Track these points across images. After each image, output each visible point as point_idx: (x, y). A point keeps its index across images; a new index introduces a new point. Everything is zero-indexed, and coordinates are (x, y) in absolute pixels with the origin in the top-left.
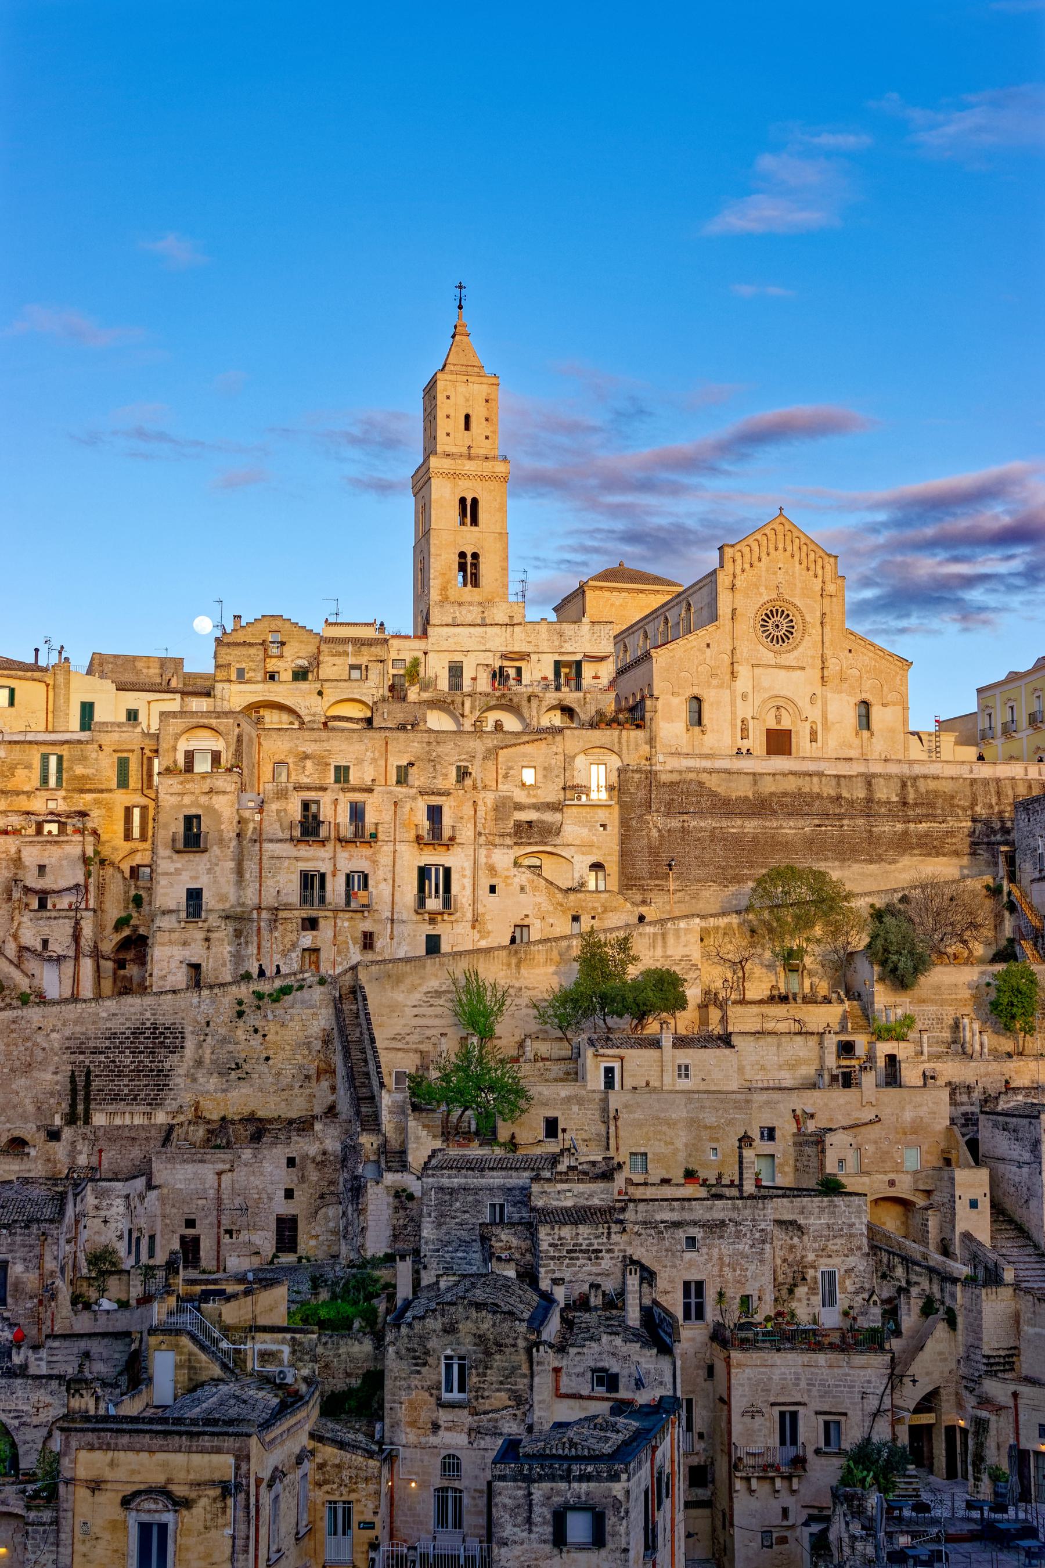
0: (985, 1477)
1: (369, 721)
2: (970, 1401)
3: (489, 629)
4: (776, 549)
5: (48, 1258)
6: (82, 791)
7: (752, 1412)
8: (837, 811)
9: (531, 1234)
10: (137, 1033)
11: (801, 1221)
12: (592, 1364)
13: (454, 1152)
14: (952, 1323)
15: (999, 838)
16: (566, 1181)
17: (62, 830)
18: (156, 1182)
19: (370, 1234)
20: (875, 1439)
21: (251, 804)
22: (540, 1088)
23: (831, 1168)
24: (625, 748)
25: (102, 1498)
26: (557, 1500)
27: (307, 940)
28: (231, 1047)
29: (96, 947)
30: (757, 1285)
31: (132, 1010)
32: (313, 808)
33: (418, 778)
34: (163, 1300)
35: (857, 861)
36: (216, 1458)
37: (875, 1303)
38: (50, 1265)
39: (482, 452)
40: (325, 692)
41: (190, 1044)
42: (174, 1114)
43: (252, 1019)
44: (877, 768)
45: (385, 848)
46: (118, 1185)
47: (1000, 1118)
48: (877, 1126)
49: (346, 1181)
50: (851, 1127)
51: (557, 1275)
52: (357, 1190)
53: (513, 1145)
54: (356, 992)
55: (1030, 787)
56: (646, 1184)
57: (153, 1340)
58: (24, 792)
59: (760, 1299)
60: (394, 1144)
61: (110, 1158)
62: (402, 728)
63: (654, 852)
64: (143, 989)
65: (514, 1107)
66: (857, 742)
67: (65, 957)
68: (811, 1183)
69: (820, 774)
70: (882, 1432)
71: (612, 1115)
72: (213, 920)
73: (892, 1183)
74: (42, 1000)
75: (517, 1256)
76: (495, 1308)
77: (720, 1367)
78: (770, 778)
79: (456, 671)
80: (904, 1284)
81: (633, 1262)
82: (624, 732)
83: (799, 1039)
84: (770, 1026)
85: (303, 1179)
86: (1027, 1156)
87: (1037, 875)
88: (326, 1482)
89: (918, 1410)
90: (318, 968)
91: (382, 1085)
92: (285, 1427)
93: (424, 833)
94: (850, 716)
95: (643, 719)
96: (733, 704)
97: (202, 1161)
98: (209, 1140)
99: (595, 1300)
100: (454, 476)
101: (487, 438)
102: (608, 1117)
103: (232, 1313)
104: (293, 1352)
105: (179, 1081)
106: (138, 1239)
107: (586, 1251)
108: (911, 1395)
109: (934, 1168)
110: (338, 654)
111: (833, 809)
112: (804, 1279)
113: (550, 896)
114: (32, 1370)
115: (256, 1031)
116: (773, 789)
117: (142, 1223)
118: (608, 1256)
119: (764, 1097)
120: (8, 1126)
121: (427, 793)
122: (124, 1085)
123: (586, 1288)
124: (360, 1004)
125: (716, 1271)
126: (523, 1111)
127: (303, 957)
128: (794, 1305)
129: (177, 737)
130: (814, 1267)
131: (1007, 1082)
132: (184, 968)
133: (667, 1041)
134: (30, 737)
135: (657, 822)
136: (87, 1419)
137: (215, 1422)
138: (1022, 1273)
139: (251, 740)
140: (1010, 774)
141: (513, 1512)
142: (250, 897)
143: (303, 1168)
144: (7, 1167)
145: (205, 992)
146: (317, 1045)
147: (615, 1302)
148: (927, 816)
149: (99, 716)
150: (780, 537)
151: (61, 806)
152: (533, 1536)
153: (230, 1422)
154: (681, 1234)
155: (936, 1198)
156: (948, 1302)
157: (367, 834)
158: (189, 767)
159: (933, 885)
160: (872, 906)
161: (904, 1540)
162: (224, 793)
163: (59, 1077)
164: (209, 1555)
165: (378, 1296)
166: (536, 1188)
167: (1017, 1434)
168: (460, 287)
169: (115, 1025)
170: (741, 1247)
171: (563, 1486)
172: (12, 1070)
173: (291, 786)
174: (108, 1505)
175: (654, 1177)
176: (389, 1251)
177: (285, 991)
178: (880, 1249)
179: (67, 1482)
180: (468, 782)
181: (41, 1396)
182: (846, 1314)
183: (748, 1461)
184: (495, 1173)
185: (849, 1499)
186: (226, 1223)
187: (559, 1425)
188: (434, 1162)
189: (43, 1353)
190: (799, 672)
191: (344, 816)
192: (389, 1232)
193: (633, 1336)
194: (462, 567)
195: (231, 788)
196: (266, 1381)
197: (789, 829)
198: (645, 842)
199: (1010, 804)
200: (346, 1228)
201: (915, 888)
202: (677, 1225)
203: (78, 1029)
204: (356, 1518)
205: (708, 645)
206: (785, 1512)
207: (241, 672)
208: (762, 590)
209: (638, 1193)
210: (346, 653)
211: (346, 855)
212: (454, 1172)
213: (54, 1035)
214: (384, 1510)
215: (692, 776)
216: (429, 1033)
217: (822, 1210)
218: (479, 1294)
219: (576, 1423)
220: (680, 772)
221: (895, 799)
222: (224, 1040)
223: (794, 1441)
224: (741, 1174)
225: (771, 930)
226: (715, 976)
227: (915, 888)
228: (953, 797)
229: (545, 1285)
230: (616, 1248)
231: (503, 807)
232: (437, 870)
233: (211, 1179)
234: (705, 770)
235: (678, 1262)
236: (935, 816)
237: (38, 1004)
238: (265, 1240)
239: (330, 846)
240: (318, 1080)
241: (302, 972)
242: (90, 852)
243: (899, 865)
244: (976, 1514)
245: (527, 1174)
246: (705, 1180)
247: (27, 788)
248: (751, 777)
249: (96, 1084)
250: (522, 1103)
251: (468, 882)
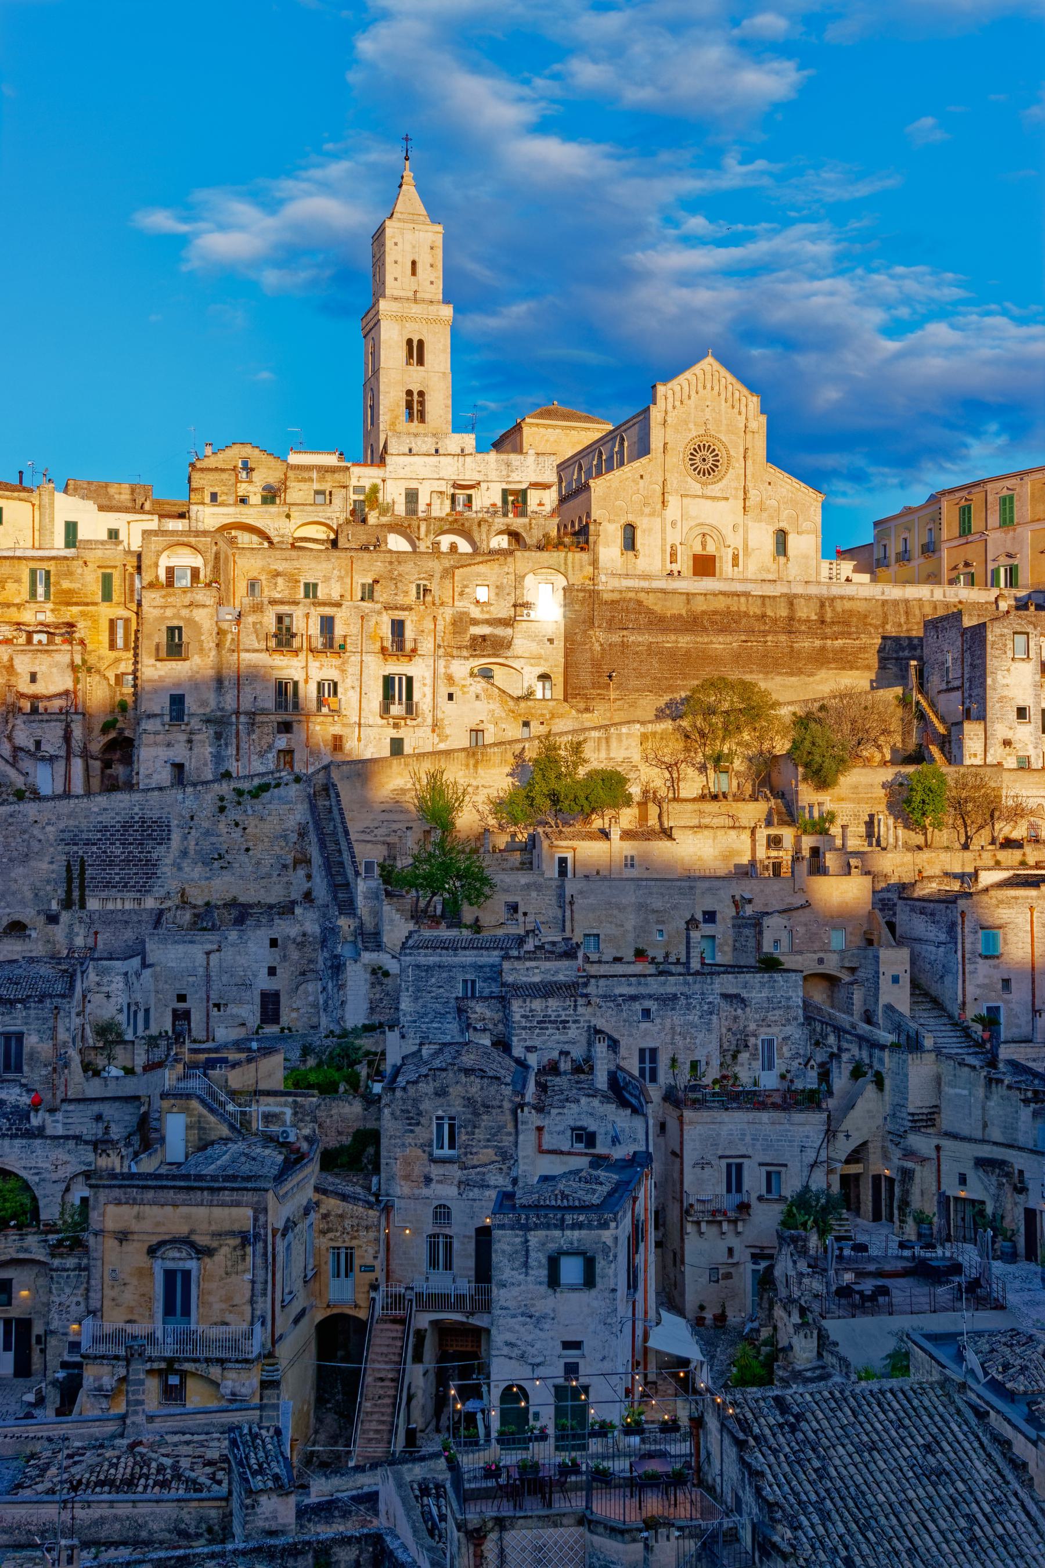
0: (910, 1220)
1: (334, 543)
2: (896, 1154)
3: (442, 458)
4: (704, 387)
5: (61, 1030)
6: (68, 604)
7: (702, 1164)
8: (762, 628)
9: (504, 1007)
10: (126, 826)
11: (745, 995)
12: (572, 1123)
13: (427, 933)
14: (879, 1082)
15: (906, 653)
16: (535, 959)
17: (50, 642)
18: (150, 960)
19: (349, 1007)
20: (814, 1188)
21: (229, 617)
22: (501, 876)
23: (767, 947)
24: (570, 569)
25: (129, 1247)
26: (552, 1246)
27: (282, 742)
28: (214, 839)
29: (85, 748)
30: (705, 1052)
31: (122, 805)
32: (287, 620)
33: (382, 594)
34: (173, 1067)
35: (779, 674)
36: (235, 1211)
37: (812, 1067)
38: (63, 1036)
39: (427, 296)
40: (292, 514)
41: (176, 837)
42: (162, 900)
43: (233, 814)
44: (799, 590)
45: (353, 658)
46: (118, 963)
47: (917, 903)
48: (807, 910)
49: (326, 959)
50: (784, 911)
51: (529, 1043)
52: (337, 967)
53: (477, 927)
54: (328, 789)
55: (935, 608)
56: (600, 962)
57: (166, 1104)
58: (14, 605)
59: (707, 1063)
60: (369, 925)
61: (105, 939)
62: (365, 548)
63: (597, 665)
64: (130, 786)
65: (479, 894)
66: (774, 567)
67: (57, 757)
68: (752, 961)
69: (747, 594)
70: (818, 1181)
71: (567, 900)
72: (195, 724)
73: (821, 961)
74: (37, 797)
75: (491, 1026)
76: (482, 1074)
77: (672, 1125)
78: (702, 598)
79: (412, 496)
80: (835, 1050)
81: (598, 1032)
82: (570, 554)
83: (733, 833)
84: (706, 821)
85: (285, 958)
86: (943, 937)
87: (944, 686)
88: (330, 1230)
89: (848, 1162)
90: (292, 767)
91: (357, 874)
92: (295, 1182)
93: (388, 644)
94: (769, 543)
95: (587, 542)
96: (663, 531)
97: (191, 942)
98: (195, 923)
99: (565, 1066)
100: (402, 319)
102: (564, 902)
103: (236, 1079)
104: (295, 1114)
105: (166, 869)
106: (135, 1013)
107: (555, 1022)
108: (843, 1148)
109: (859, 948)
110: (304, 480)
111: (758, 626)
112: (747, 1046)
113: (503, 703)
114: (49, 1132)
115: (237, 825)
116: (704, 608)
117: (138, 997)
118: (574, 1026)
119: (706, 884)
120: (8, 910)
121: (391, 608)
122: (115, 874)
123: (555, 1054)
124: (333, 800)
125: (668, 1039)
126: (487, 897)
127: (278, 758)
128: (737, 1069)
129: (159, 554)
130: (755, 1036)
131: (920, 872)
132: (169, 768)
133: (615, 834)
134: (18, 553)
136: (113, 1176)
137: (234, 1178)
138: (940, 1040)
139: (227, 558)
140: (917, 596)
141: (511, 1258)
142: (229, 702)
143: (285, 948)
144: (10, 948)
145: (189, 789)
146: (293, 837)
147: (583, 1067)
148: (842, 633)
149: (82, 534)
150: (708, 376)
151: (49, 617)
152: (529, 1278)
153: (248, 1179)
154: (637, 1006)
155: (861, 974)
156: (877, 1066)
157: (336, 645)
158: (170, 582)
159: (851, 696)
160: (794, 714)
161: (848, 1277)
162: (204, 606)
163: (54, 867)
164: (231, 1298)
165: (360, 1062)
166: (506, 965)
167: (939, 1182)
169: (105, 818)
170: (691, 1018)
171: (557, 1233)
172: (10, 860)
173: (266, 601)
174: (135, 1255)
175: (608, 954)
176: (367, 1022)
177: (264, 788)
178: (815, 1019)
179: (96, 1234)
180: (429, 598)
181: (60, 1154)
182: (783, 1077)
183: (698, 1207)
184: (467, 953)
185: (794, 1240)
186: (214, 997)
187: (545, 1179)
188: (411, 942)
189: (59, 1116)
190: (723, 503)
191: (315, 628)
192: (366, 1006)
193: (606, 1099)
194: (409, 406)
195: (210, 601)
196: (269, 1139)
197: (719, 644)
198: (588, 655)
199: (918, 623)
200: (326, 1002)
201: (835, 697)
202: (634, 998)
203: (71, 823)
204: (357, 1262)
206: (731, 1251)
207: (214, 497)
208: (691, 426)
209: (593, 970)
210: (311, 480)
211: (317, 664)
212: (430, 951)
213: (49, 828)
214: (382, 1255)
215: (632, 595)
216: (395, 826)
217: (763, 985)
218: (468, 1059)
219: (564, 1175)
220: (621, 592)
221: (814, 617)
222: (207, 833)
223: (739, 1189)
224: (688, 953)
225: (703, 735)
226: (656, 778)
227: (835, 697)
228: (866, 617)
229: (518, 1051)
230: (582, 1019)
231: (461, 622)
232: (400, 679)
233: (201, 958)
234: (643, 590)
235: (634, 1031)
236: (850, 634)
237: (33, 800)
238: (250, 1012)
239: (302, 656)
240: (295, 869)
241: (280, 771)
242: (78, 661)
243: (817, 678)
244: (907, 1253)
245: (496, 953)
246: (653, 958)
247: (17, 601)
249: (89, 872)
250: (486, 890)
251: (428, 691)
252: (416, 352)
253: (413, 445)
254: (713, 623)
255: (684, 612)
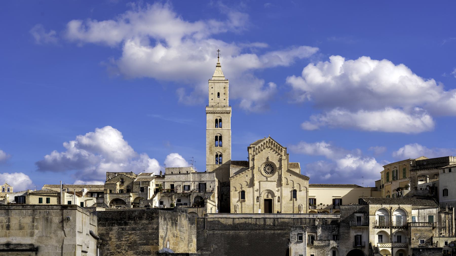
3: (182, 176)
24: (199, 212)
69: (251, 218)
82: (199, 209)
101: (224, 99)
135: (208, 232)
168: (219, 51)
190: (274, 182)
205: (247, 176)
208: (264, 159)
215: (217, 219)
220: (213, 218)
221: (272, 224)
228: (288, 223)
234: (220, 218)
248: (232, 219)
252: (218, 122)
253: (173, 171)
254: (240, 227)
255: (232, 224)
